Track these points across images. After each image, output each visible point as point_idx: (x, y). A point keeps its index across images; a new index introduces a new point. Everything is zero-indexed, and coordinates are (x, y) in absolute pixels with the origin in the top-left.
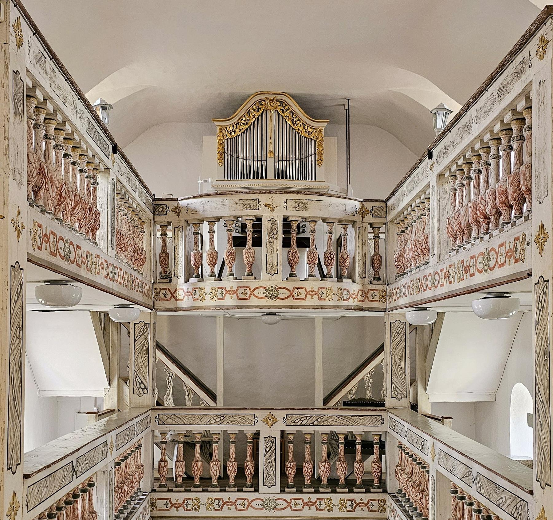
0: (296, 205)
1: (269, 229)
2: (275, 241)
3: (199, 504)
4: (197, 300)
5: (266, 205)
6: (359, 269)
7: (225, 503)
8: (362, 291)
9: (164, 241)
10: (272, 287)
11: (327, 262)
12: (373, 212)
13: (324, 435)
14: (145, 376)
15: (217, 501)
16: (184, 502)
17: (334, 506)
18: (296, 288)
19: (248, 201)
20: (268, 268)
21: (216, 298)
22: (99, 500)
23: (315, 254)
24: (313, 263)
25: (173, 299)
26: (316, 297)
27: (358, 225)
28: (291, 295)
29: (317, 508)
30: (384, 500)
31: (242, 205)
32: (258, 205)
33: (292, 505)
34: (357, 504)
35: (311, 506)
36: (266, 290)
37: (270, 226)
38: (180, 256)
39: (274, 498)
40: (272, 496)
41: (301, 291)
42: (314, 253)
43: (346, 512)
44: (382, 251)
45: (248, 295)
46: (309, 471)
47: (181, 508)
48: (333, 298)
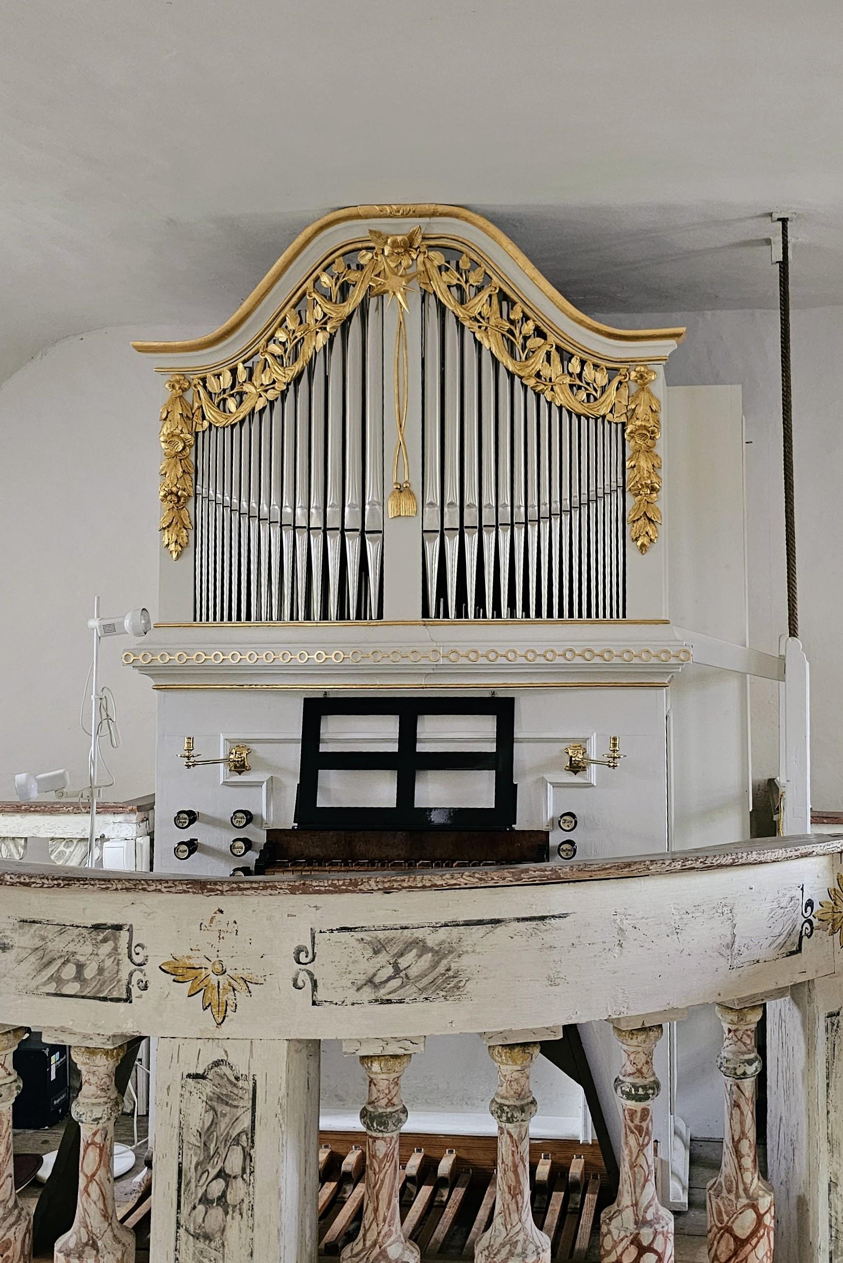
0: (382, 965)
1: (193, 1140)
2: (235, 1227)
19: (66, 937)
31: (32, 959)
32: (127, 967)
37: (198, 1116)
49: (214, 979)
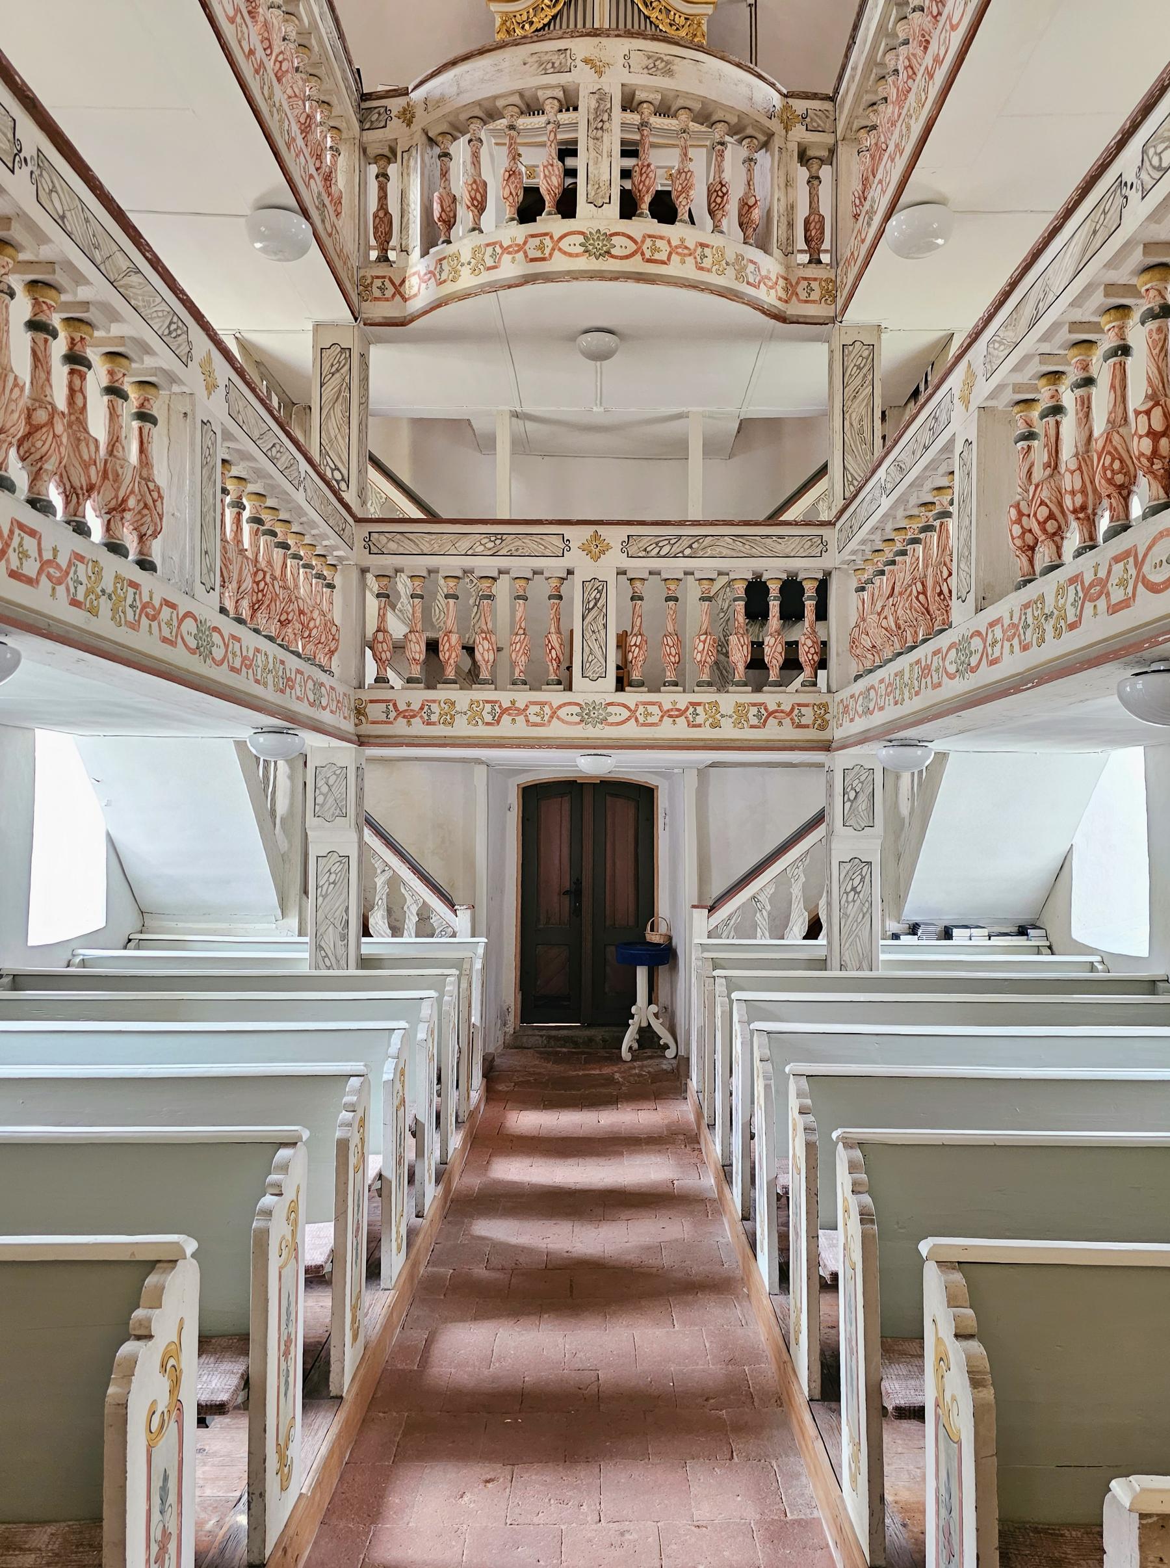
0: (650, 63)
2: (605, 135)
3: (453, 713)
4: (445, 281)
5: (586, 61)
6: (780, 232)
7: (505, 711)
8: (786, 279)
9: (383, 189)
10: (598, 231)
11: (715, 201)
12: (808, 120)
13: (704, 582)
14: (343, 457)
15: (488, 707)
16: (422, 709)
17: (722, 716)
18: (650, 236)
20: (589, 191)
21: (482, 267)
22: (175, 479)
23: (689, 174)
24: (684, 195)
25: (398, 297)
26: (690, 260)
27: (777, 142)
28: (638, 251)
29: (688, 721)
30: (825, 706)
32: (569, 61)
33: (638, 716)
34: (770, 714)
35: (677, 717)
36: (586, 238)
37: (593, 104)
38: (412, 206)
39: (603, 701)
40: (599, 698)
41: (659, 243)
42: (686, 173)
43: (747, 730)
44: (825, 209)
45: (547, 251)
46: (673, 652)
47: (418, 719)
48: (726, 272)
49: (598, 63)
